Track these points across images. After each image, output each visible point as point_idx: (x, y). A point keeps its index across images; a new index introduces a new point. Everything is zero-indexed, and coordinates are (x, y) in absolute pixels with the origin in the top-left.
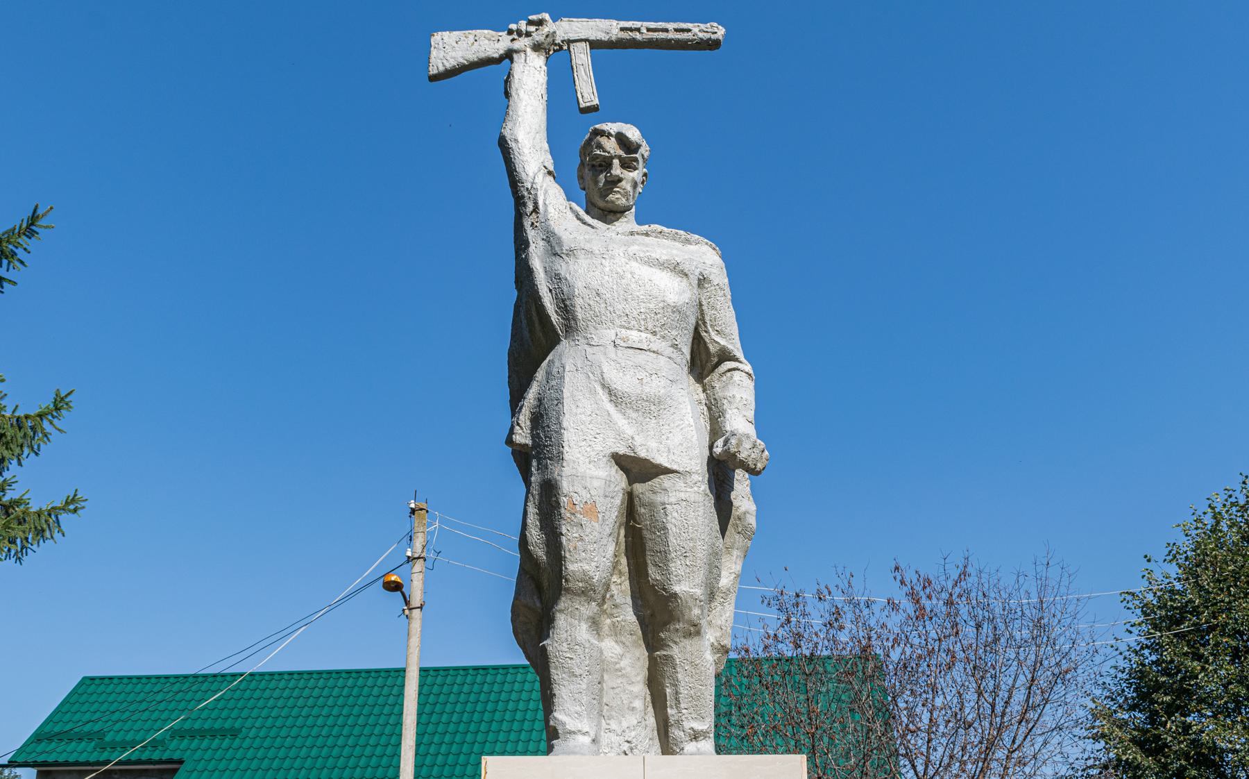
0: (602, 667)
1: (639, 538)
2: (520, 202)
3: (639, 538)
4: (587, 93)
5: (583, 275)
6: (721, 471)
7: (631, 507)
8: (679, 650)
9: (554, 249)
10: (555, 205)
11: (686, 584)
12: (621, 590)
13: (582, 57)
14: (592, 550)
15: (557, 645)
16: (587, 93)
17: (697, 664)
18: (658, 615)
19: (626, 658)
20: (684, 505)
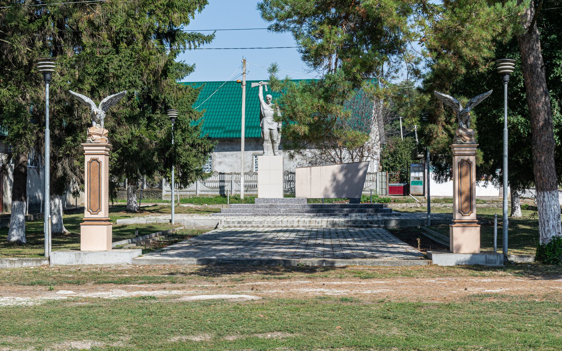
0: (268, 146)
1: (271, 135)
2: (260, 103)
3: (271, 135)
4: (267, 90)
5: (265, 112)
6: (278, 129)
7: (270, 132)
8: (275, 145)
9: (263, 109)
10: (263, 102)
11: (275, 139)
12: (270, 139)
13: (266, 86)
14: (267, 137)
15: (264, 145)
16: (267, 90)
17: (277, 145)
18: (273, 142)
19: (271, 145)
20: (275, 133)
